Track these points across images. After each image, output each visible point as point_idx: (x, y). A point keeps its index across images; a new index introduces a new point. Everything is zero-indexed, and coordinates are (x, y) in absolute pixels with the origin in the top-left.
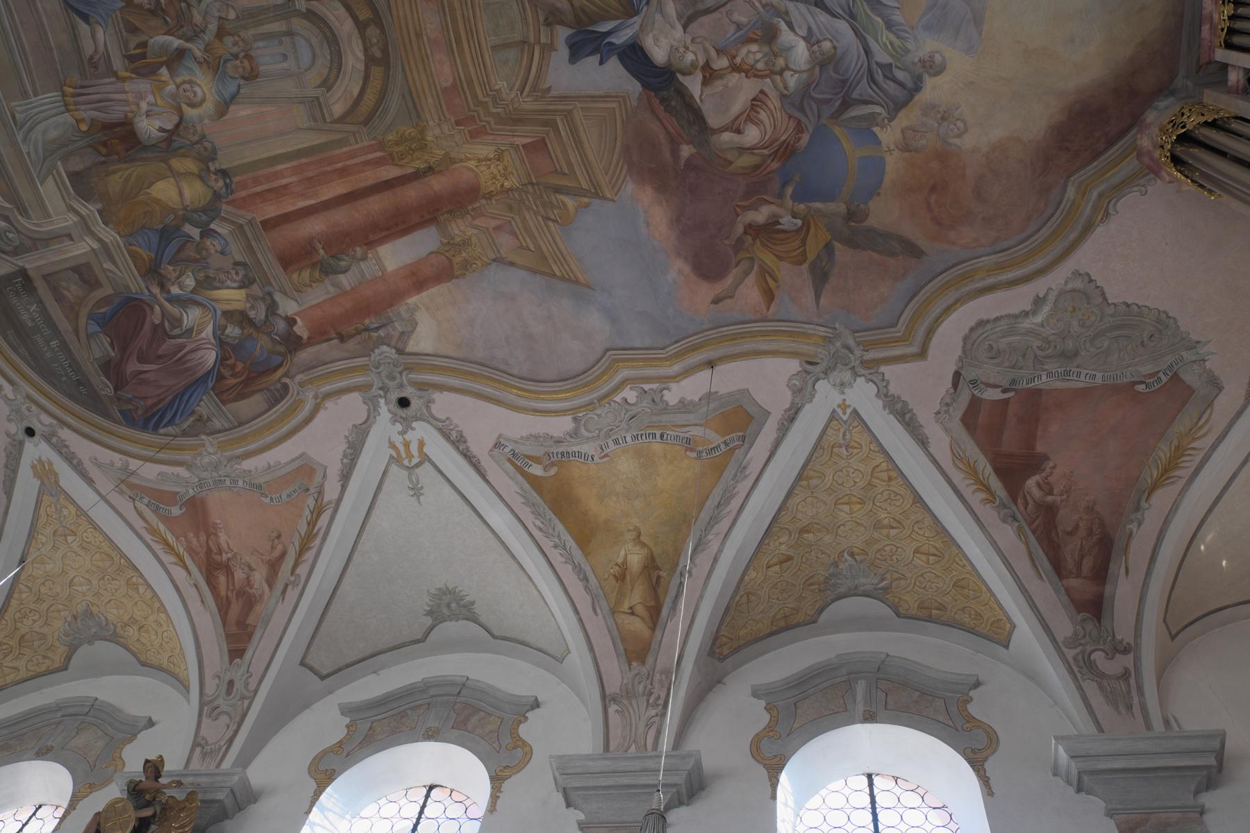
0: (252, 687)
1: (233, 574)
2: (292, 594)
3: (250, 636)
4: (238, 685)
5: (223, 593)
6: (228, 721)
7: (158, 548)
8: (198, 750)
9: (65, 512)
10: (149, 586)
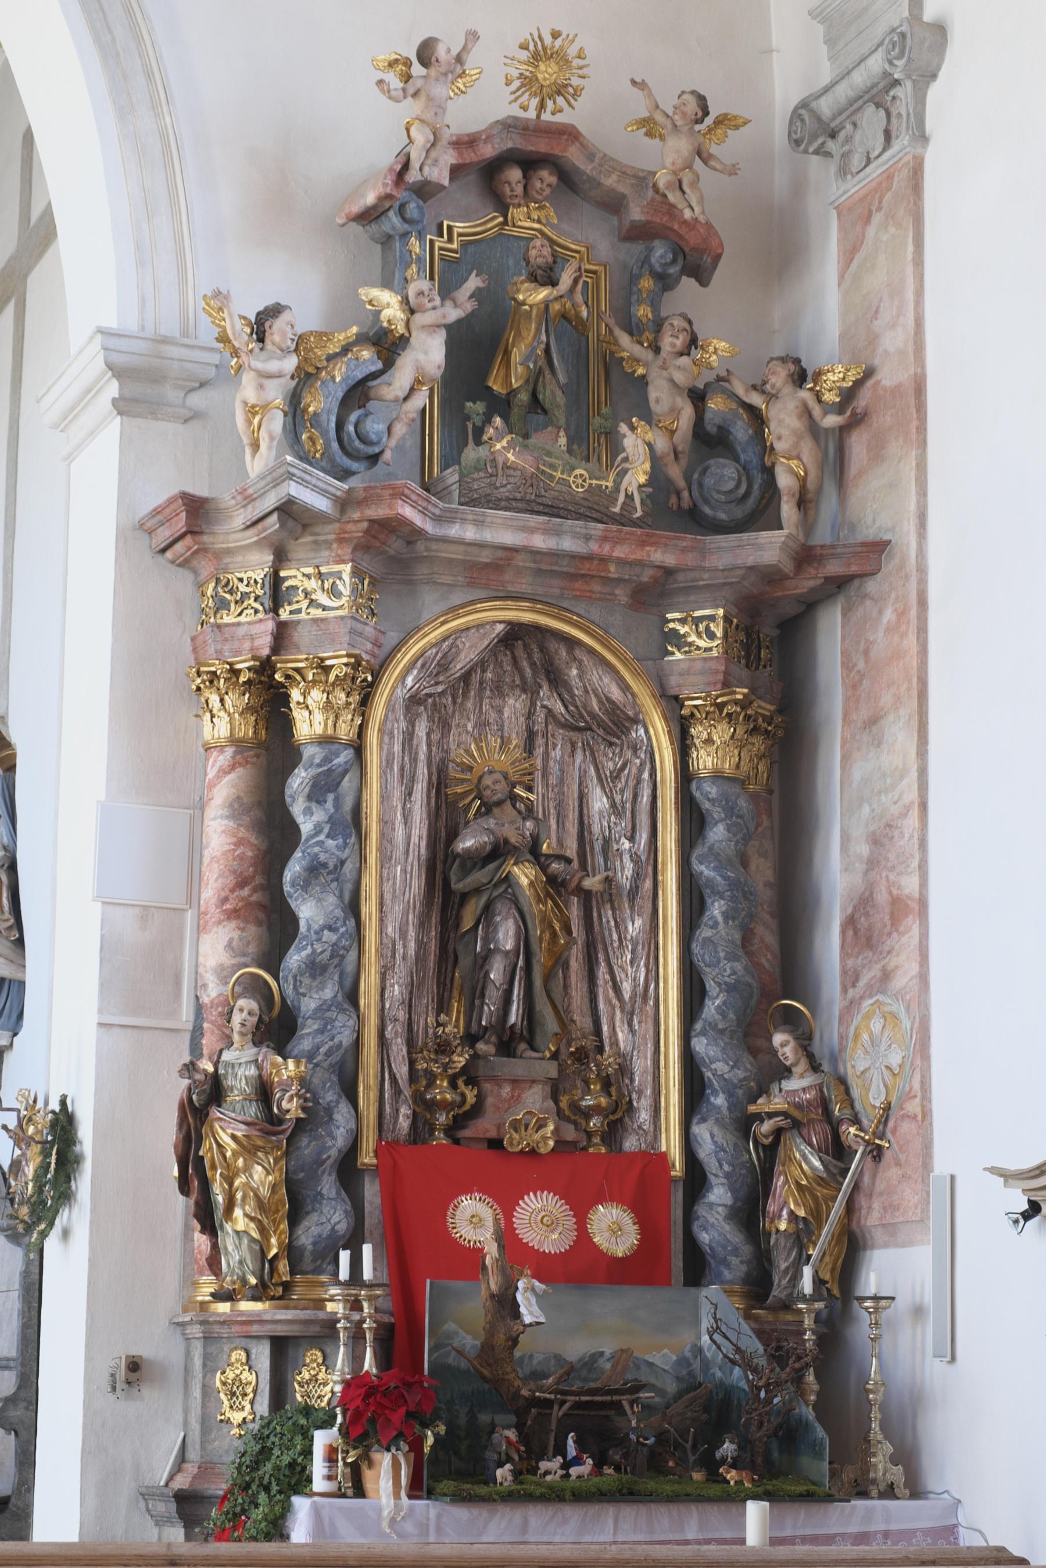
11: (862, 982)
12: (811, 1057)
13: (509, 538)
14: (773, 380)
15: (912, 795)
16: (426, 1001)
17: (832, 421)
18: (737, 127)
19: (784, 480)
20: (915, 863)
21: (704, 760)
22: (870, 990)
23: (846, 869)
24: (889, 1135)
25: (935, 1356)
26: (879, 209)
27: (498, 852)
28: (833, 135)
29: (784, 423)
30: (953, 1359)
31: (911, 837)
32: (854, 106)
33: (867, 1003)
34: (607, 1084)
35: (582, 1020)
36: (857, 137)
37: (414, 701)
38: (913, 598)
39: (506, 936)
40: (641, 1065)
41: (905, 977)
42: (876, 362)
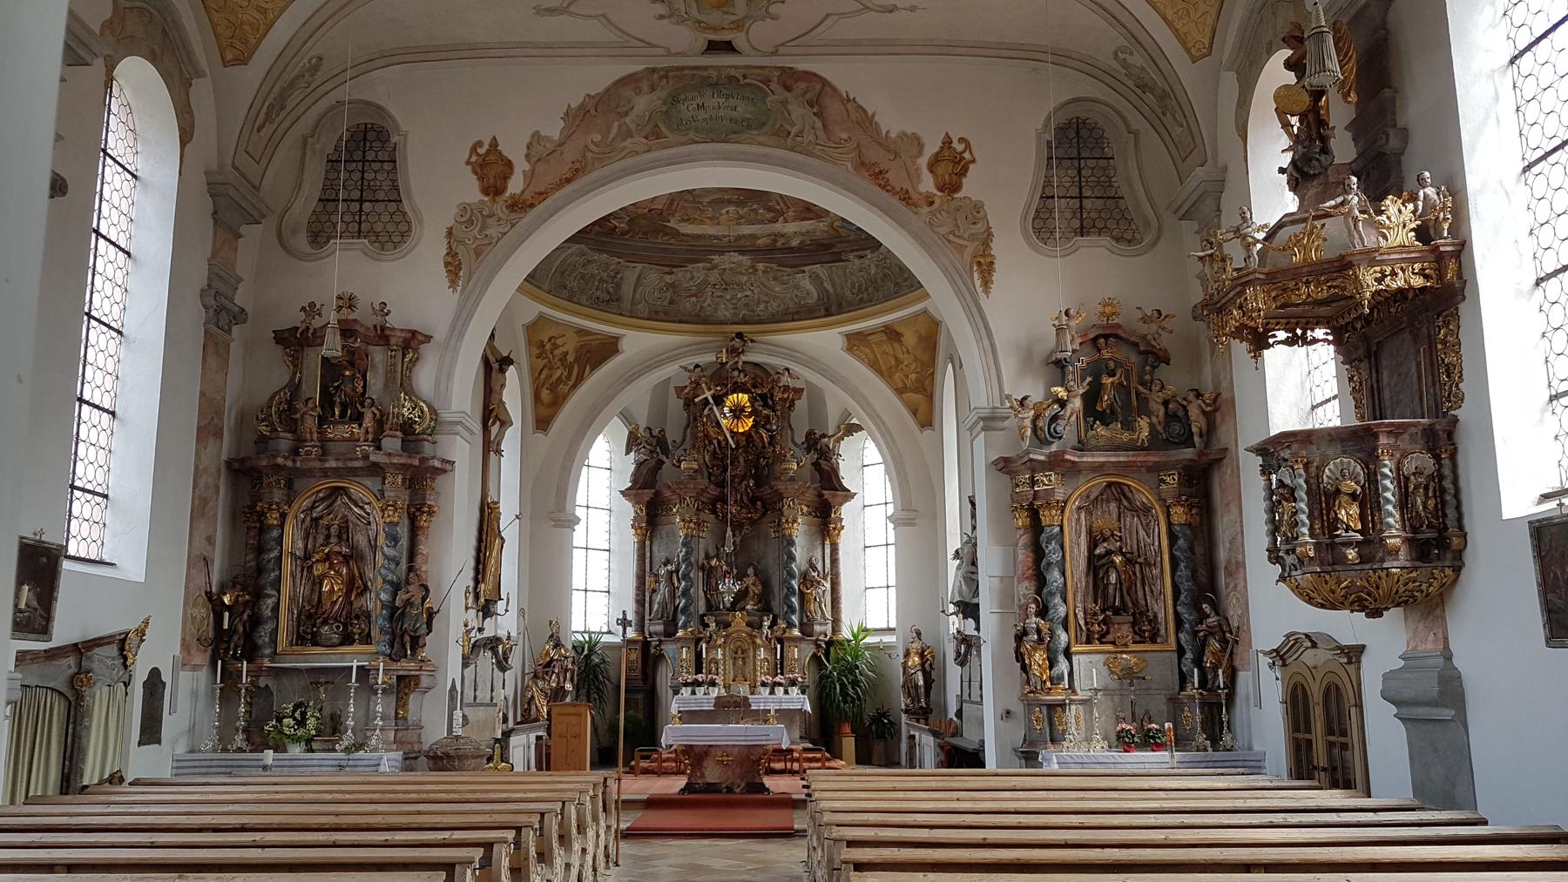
13: (1102, 459)
16: (1090, 599)
21: (1175, 520)
27: (1109, 553)
34: (1150, 622)
35: (1142, 602)
37: (1079, 508)
39: (1113, 578)
40: (1161, 616)
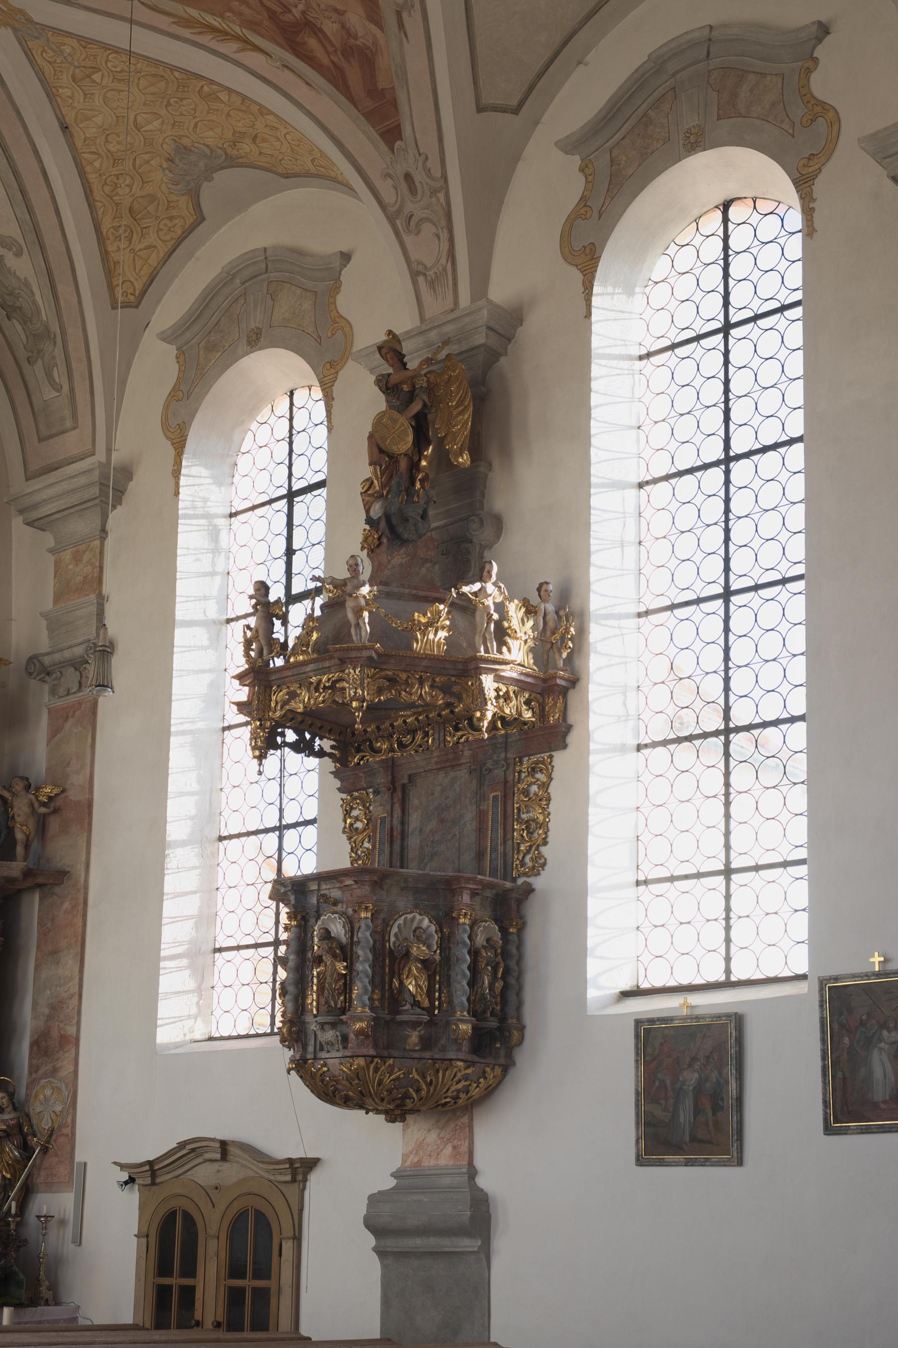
0: (437, 173)
1: (321, 30)
2: (413, 22)
3: (394, 103)
4: (419, 177)
5: (326, 61)
6: (434, 229)
7: (205, 39)
8: (421, 279)
9: (68, 50)
10: (230, 90)
11: (41, 1072)
12: (13, 1104)
14: (17, 787)
15: (76, 990)
17: (43, 810)
18: (6, 665)
19: (19, 836)
20: (75, 1021)
22: (45, 1076)
23: (35, 1018)
24: (52, 1142)
25: (73, 1242)
26: (73, 716)
28: (48, 674)
29: (21, 808)
30: (80, 1244)
31: (73, 1009)
32: (63, 664)
33: (43, 1081)
36: (63, 680)
38: (81, 900)
41: (66, 1071)
42: (66, 787)
